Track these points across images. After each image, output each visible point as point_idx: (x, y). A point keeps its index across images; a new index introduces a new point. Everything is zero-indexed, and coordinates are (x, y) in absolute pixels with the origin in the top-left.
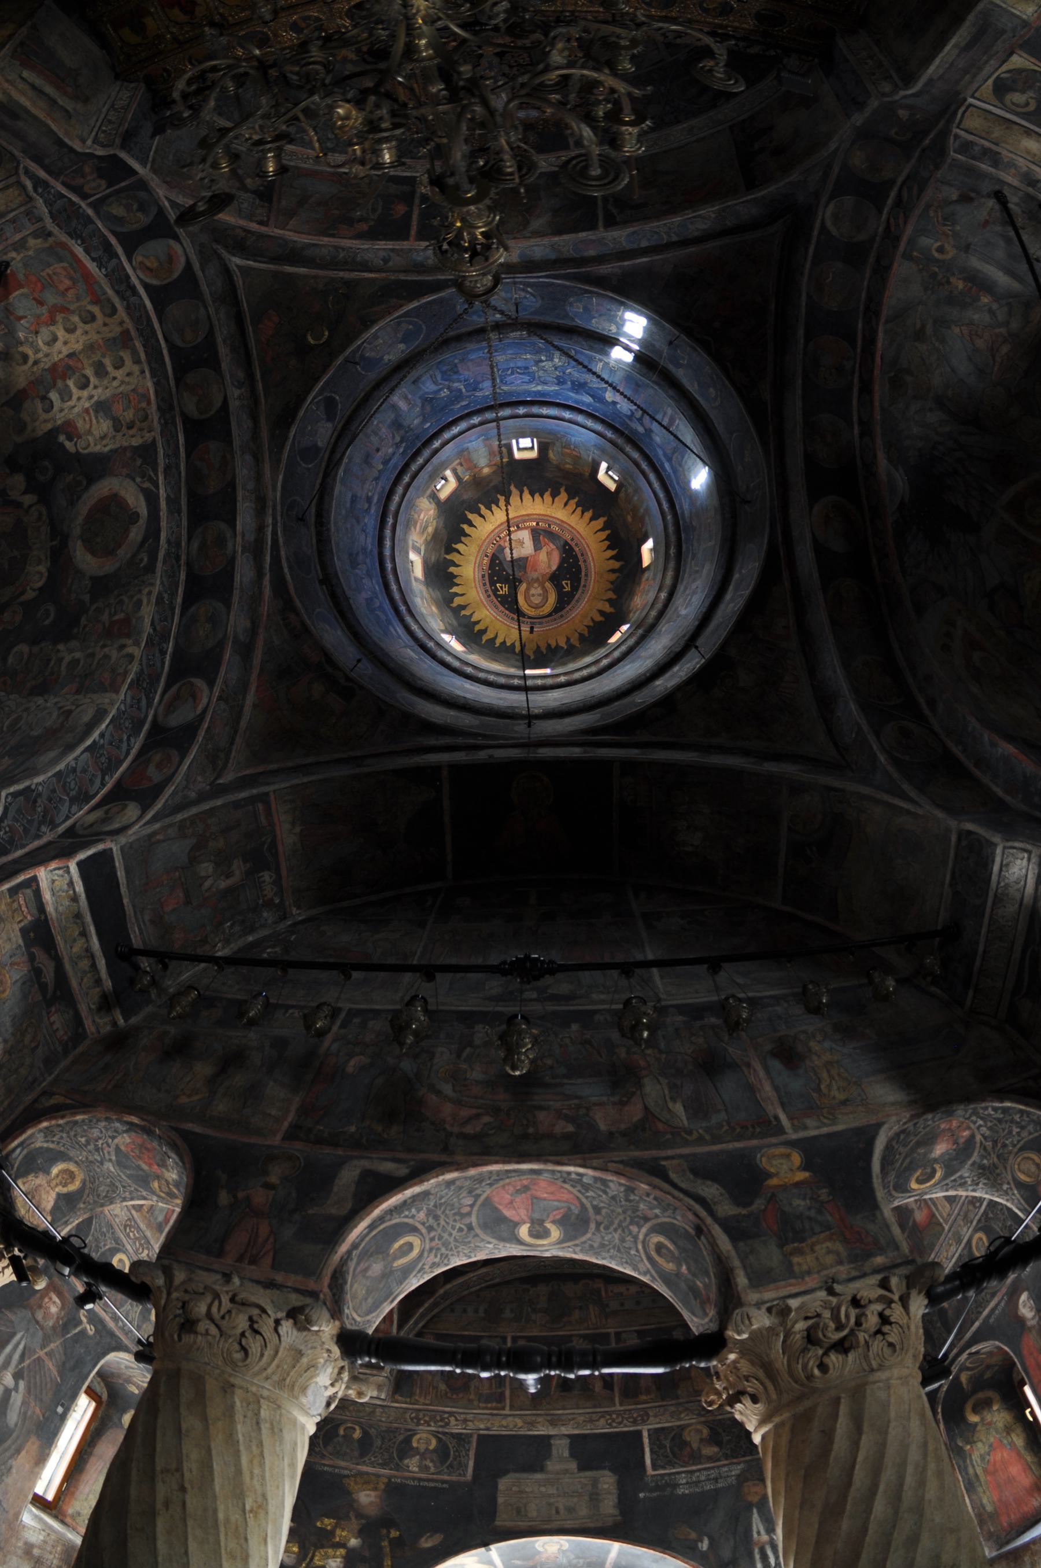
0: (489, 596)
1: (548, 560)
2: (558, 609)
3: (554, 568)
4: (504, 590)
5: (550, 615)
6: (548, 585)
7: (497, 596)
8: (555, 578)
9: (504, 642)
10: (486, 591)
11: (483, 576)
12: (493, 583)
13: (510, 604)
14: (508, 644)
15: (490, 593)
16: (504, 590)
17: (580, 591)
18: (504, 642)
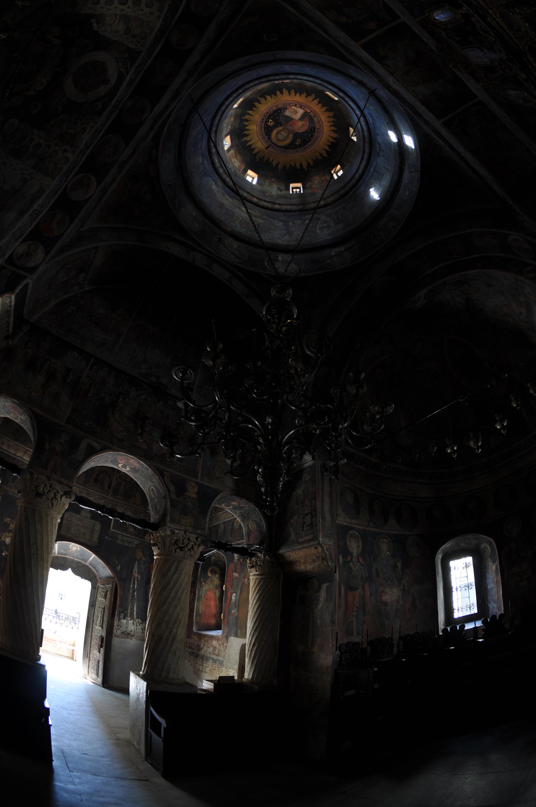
0: (262, 122)
1: (301, 127)
2: (286, 147)
3: (300, 131)
4: (271, 123)
5: (281, 147)
6: (291, 135)
7: (266, 124)
8: (296, 135)
9: (251, 145)
10: (263, 119)
11: (267, 113)
12: (269, 118)
13: (268, 131)
14: (252, 147)
15: (264, 121)
16: (271, 123)
17: (301, 149)
18: (251, 145)
